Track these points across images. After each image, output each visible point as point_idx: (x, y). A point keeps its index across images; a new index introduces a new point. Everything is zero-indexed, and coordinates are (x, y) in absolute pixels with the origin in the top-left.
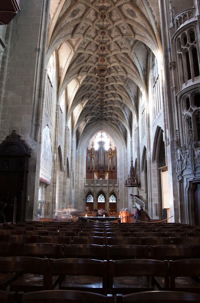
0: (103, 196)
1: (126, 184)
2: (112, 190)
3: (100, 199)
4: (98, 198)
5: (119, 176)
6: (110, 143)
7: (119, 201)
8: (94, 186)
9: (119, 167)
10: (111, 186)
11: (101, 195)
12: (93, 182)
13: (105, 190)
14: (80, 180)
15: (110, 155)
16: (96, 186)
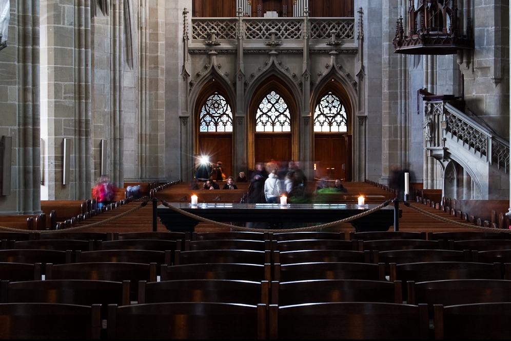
1: (399, 40)
2: (325, 72)
3: (264, 118)
4: (259, 113)
7: (361, 125)
8: (232, 54)
10: (325, 53)
11: (273, 96)
12: (229, 31)
13: (293, 68)
14: (160, 20)
16: (248, 53)
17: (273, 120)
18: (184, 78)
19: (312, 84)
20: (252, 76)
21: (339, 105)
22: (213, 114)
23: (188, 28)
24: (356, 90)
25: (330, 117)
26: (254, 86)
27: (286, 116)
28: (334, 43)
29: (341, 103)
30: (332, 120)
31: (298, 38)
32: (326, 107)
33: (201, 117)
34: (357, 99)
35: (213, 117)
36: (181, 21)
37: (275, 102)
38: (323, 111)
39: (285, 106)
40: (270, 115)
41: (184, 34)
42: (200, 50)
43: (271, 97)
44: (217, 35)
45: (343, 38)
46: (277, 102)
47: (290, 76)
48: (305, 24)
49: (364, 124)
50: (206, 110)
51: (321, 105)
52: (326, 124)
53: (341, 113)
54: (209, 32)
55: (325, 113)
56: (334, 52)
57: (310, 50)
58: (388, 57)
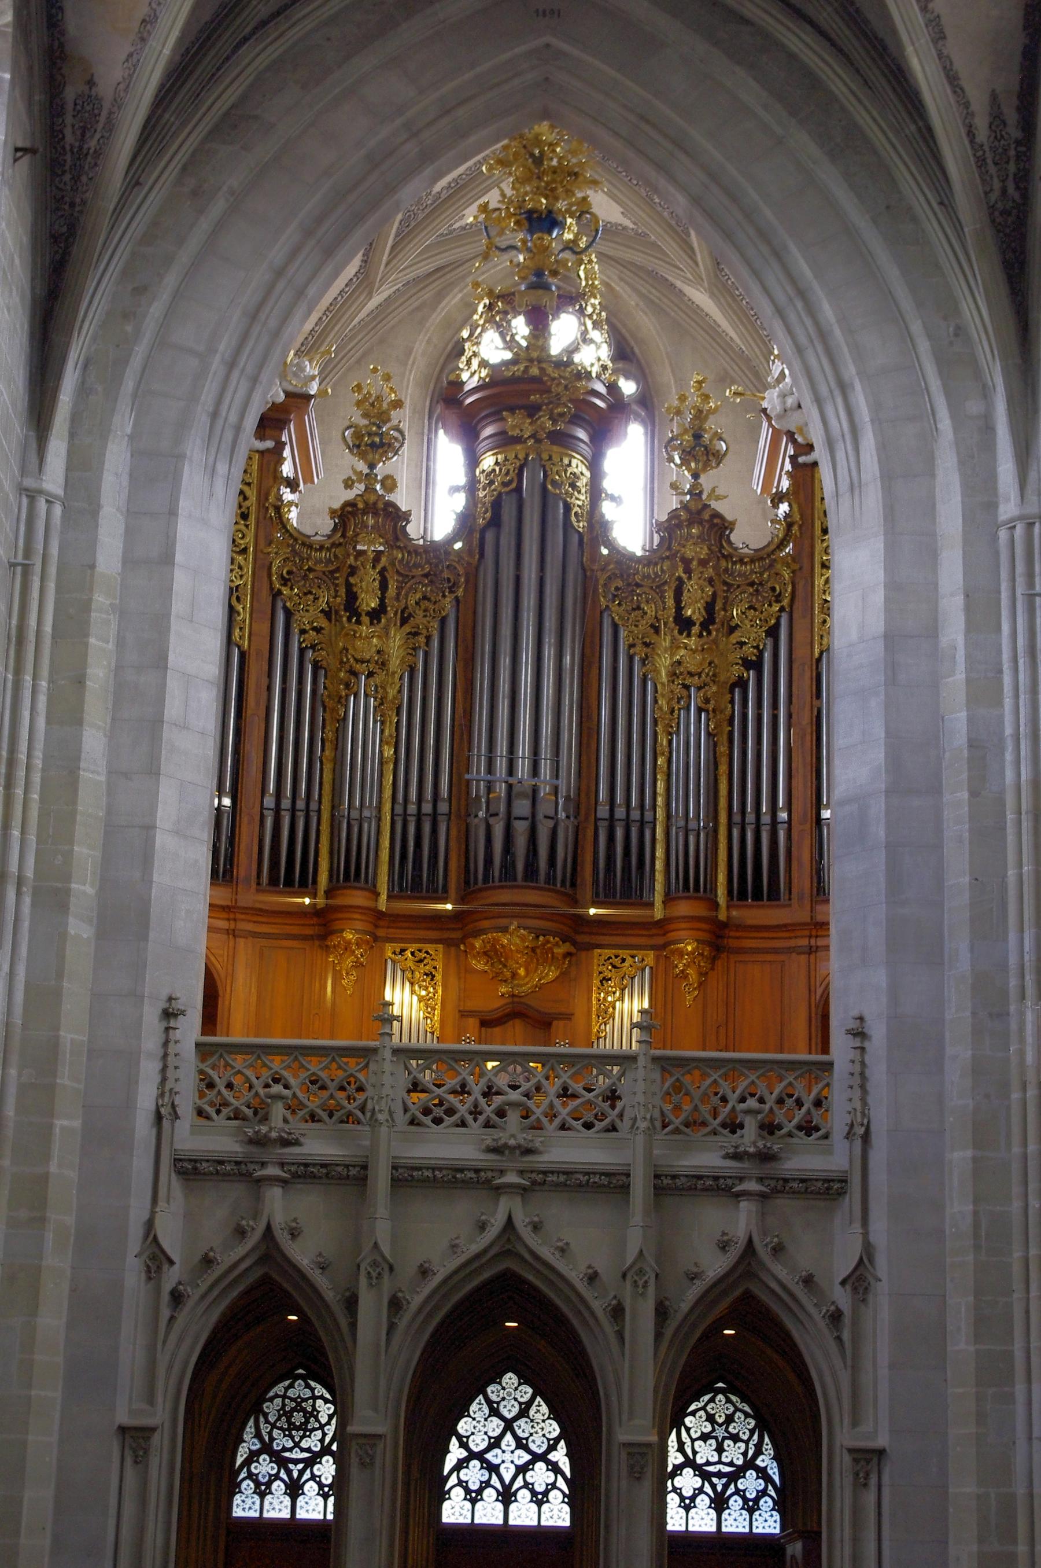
0: (541, 1409)
3: (474, 1474)
4: (455, 1453)
5: (880, 977)
6: (700, 415)
7: (860, 1483)
9: (878, 808)
15: (684, 624)
17: (507, 1479)
18: (149, 1270)
19: (662, 1312)
20: (424, 1272)
21: (752, 1432)
22: (285, 1449)
23: (180, 1074)
24: (839, 1339)
25: (719, 1475)
26: (430, 1315)
27: (555, 1468)
28: (752, 1150)
29: (762, 1426)
30: (726, 1487)
31: (613, 1128)
32: (704, 1437)
33: (239, 1461)
34: (845, 1377)
35: (282, 1462)
36: (151, 1042)
37: (515, 1411)
38: (695, 1453)
39: (553, 1429)
40: (496, 1461)
41: (162, 1095)
42: (221, 1163)
43: (502, 1393)
44: (293, 1107)
45: (790, 1135)
46: (524, 1412)
47: (575, 1275)
48: (641, 1073)
49: (873, 1480)
50: (258, 1435)
51: (688, 1430)
52: (703, 1501)
53: (759, 1462)
54: (262, 1092)
55: (699, 1460)
56: (752, 1186)
57: (657, 1177)
58: (971, 1207)
